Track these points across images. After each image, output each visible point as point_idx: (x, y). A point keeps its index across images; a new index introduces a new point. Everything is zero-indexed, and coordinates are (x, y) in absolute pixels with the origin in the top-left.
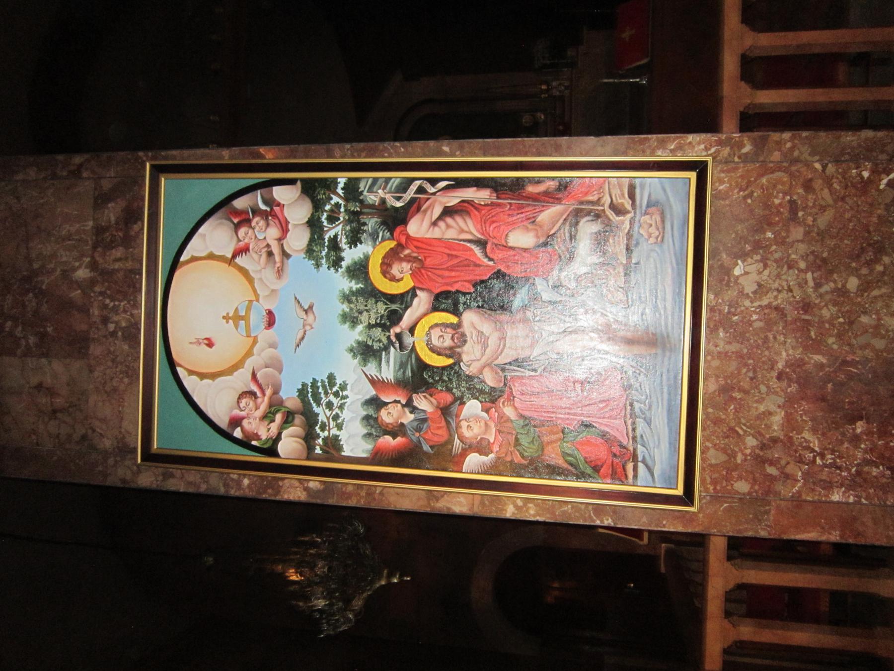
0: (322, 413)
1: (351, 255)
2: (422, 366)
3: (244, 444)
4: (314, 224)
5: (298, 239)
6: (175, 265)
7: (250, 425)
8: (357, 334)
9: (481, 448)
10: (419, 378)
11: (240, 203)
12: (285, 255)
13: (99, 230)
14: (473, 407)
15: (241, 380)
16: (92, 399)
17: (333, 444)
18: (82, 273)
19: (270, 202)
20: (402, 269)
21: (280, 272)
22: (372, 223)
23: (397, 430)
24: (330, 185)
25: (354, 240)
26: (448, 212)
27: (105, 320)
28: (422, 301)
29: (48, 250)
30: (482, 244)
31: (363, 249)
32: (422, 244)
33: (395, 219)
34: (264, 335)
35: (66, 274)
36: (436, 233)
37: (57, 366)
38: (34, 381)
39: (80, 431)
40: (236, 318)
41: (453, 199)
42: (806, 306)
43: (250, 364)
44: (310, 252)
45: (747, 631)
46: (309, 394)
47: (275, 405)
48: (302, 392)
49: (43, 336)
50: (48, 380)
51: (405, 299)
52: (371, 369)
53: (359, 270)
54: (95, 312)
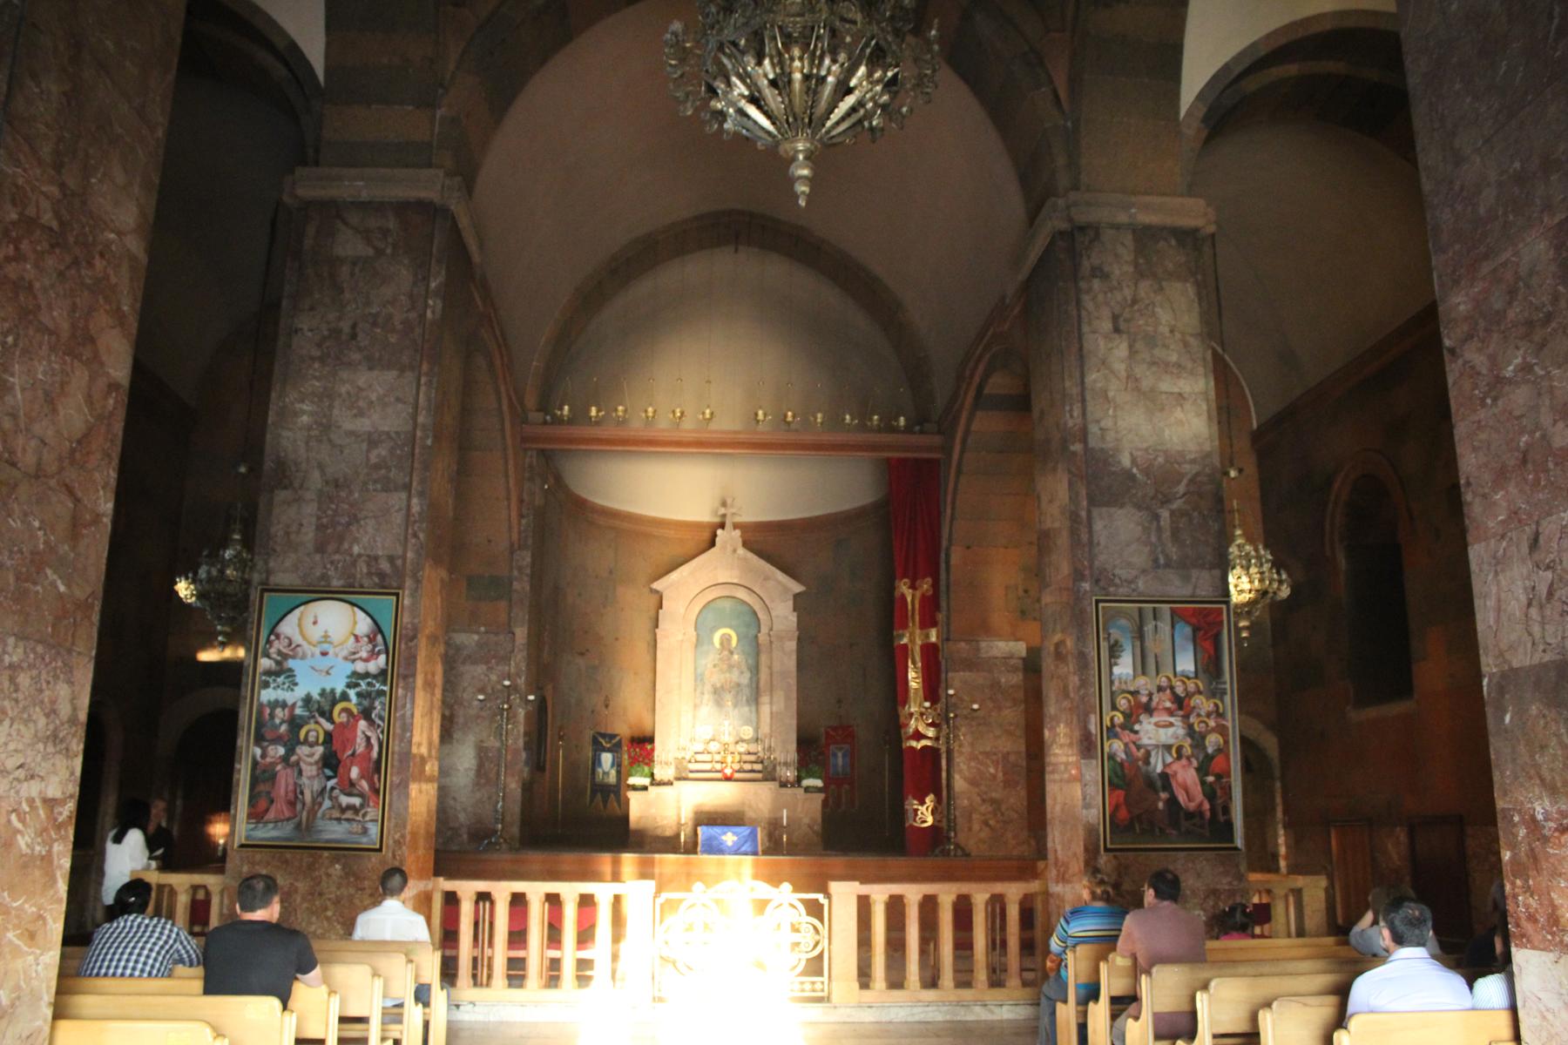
0: (280, 680)
1: (352, 693)
2: (301, 727)
3: (268, 641)
4: (367, 675)
5: (360, 667)
6: (353, 604)
7: (276, 644)
8: (316, 696)
9: (264, 756)
10: (295, 724)
11: (379, 637)
12: (353, 661)
13: (376, 558)
14: (282, 751)
15: (298, 639)
16: (293, 556)
17: (266, 685)
18: (356, 549)
19: (379, 653)
20: (344, 718)
21: (346, 658)
22: (366, 703)
23: (272, 716)
24: (384, 683)
25: (359, 695)
26: (368, 739)
27: (332, 563)
28: (329, 727)
29: (370, 530)
30: (353, 755)
31: (354, 698)
32: (355, 727)
33: (366, 714)
34: (317, 651)
35: (356, 540)
36: (359, 733)
37: (311, 535)
38: (305, 522)
39: (278, 549)
40: (326, 636)
41: (374, 741)
42: (321, 894)
43: (304, 644)
44: (354, 674)
45: (183, 900)
46: (290, 674)
47: (285, 657)
48: (291, 670)
49: (326, 527)
50: (303, 530)
51: (330, 720)
52: (300, 703)
53: (345, 697)
54: (337, 557)
